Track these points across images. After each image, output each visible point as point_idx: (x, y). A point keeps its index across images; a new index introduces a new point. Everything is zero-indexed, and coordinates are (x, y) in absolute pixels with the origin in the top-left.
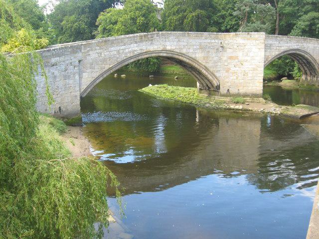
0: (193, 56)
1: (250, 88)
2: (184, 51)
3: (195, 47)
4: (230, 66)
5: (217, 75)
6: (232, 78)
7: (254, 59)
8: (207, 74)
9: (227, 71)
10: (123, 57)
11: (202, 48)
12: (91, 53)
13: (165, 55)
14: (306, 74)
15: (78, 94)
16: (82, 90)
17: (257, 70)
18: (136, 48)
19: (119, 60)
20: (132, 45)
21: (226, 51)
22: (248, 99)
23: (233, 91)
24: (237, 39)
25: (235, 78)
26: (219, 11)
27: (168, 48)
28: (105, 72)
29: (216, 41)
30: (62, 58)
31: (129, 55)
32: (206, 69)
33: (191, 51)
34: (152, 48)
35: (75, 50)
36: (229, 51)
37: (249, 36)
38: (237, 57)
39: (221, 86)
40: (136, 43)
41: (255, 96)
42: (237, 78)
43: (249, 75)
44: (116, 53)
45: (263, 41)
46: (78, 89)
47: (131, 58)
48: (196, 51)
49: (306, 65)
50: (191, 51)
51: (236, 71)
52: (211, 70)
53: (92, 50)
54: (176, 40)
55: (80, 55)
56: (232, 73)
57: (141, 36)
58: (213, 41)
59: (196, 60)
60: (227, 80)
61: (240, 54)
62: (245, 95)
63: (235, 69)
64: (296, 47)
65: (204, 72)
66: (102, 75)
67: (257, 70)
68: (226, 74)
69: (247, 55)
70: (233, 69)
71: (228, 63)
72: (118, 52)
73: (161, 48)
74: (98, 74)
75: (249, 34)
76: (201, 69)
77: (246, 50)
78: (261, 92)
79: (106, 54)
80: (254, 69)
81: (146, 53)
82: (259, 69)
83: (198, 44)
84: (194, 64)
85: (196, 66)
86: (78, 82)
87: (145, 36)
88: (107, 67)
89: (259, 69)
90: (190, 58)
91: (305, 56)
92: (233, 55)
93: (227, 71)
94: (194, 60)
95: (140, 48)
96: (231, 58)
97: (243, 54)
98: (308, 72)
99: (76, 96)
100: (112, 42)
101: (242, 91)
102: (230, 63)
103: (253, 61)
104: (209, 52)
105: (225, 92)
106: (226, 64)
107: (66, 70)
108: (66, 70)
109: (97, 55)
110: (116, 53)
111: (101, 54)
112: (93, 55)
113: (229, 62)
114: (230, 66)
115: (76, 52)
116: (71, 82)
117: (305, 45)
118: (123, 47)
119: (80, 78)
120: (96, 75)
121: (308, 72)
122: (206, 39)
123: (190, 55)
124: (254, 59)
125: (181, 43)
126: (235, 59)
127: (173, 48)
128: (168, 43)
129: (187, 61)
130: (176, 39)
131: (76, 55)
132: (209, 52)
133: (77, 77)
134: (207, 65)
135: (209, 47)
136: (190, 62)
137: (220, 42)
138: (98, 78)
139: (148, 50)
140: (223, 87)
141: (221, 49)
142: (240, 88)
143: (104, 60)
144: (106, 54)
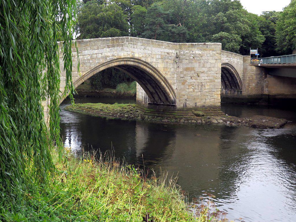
0: (156, 66)
1: (208, 101)
2: (149, 60)
3: (157, 57)
4: (186, 78)
5: (174, 87)
8: (165, 86)
9: (183, 84)
11: (163, 58)
18: (109, 54)
19: (93, 66)
24: (193, 49)
25: (191, 90)
27: (136, 56)
32: (166, 81)
34: (123, 54)
36: (185, 62)
37: (205, 47)
38: (192, 69)
40: (109, 47)
42: (194, 91)
43: (207, 87)
44: (89, 58)
47: (103, 65)
48: (158, 61)
49: (228, 80)
50: (154, 60)
51: (192, 84)
52: (170, 81)
54: (142, 47)
56: (189, 86)
58: (171, 51)
59: (157, 71)
60: (183, 93)
61: (196, 65)
63: (191, 81)
64: (227, 61)
65: (163, 83)
68: (182, 86)
69: (204, 66)
70: (189, 81)
71: (185, 75)
72: (91, 56)
76: (161, 81)
78: (219, 104)
80: (212, 81)
81: (118, 60)
82: (216, 81)
85: (157, 77)
89: (216, 81)
91: (230, 70)
92: (189, 66)
93: (183, 84)
95: (112, 54)
96: (187, 69)
97: (199, 65)
102: (185, 74)
103: (210, 73)
105: (182, 105)
106: (182, 76)
110: (89, 58)
113: (185, 73)
114: (186, 78)
118: (96, 51)
122: (165, 48)
123: (153, 65)
125: (146, 51)
126: (190, 71)
127: (141, 56)
128: (136, 50)
129: (151, 71)
130: (142, 46)
134: (166, 77)
136: (152, 73)
137: (176, 52)
140: (180, 101)
141: (177, 60)
142: (198, 101)
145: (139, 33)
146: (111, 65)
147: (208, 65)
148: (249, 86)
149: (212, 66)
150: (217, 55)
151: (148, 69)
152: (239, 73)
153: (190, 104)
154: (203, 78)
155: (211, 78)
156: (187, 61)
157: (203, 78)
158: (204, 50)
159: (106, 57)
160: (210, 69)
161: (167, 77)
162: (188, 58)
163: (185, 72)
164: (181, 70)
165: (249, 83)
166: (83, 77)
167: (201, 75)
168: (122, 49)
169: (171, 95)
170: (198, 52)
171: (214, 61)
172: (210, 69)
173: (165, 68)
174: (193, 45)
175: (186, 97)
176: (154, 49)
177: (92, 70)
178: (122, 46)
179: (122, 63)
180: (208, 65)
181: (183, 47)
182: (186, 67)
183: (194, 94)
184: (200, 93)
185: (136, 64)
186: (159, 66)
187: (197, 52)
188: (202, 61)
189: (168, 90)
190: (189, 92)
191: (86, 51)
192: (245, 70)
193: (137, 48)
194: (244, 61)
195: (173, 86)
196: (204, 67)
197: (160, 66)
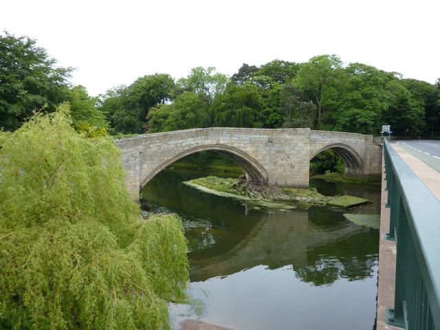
0: (244, 150)
1: (297, 180)
2: (236, 145)
3: (245, 142)
4: (277, 159)
7: (300, 153)
8: (256, 166)
10: (181, 150)
11: (252, 142)
12: (151, 146)
13: (218, 148)
14: (348, 166)
15: (138, 183)
16: (142, 180)
20: (189, 140)
22: (294, 190)
23: (281, 182)
26: (264, 108)
27: (222, 142)
28: (164, 164)
29: (265, 136)
30: (124, 151)
31: (186, 148)
32: (256, 162)
33: (242, 145)
35: (136, 143)
36: (276, 145)
38: (284, 151)
39: (269, 179)
43: (296, 168)
46: (138, 178)
47: (188, 151)
49: (349, 159)
50: (242, 145)
53: (152, 143)
55: (141, 148)
56: (280, 166)
57: (197, 131)
58: (262, 136)
60: (275, 172)
61: (287, 148)
62: (294, 187)
64: (338, 142)
65: (254, 164)
66: (160, 166)
70: (280, 162)
72: (176, 145)
73: (215, 142)
74: (157, 165)
76: (251, 162)
77: (292, 145)
79: (164, 146)
80: (301, 162)
82: (305, 162)
83: (248, 139)
84: (245, 158)
85: (247, 159)
86: (138, 172)
87: (200, 131)
88: (166, 159)
89: (305, 162)
90: (241, 152)
92: (281, 149)
94: (245, 154)
96: (278, 152)
98: (350, 164)
99: (136, 186)
100: (172, 137)
101: (289, 182)
104: (258, 146)
106: (274, 157)
107: (128, 161)
108: (128, 161)
109: (157, 148)
111: (160, 146)
112: (154, 148)
114: (277, 159)
115: (138, 145)
116: (132, 172)
117: (347, 140)
118: (181, 141)
119: (141, 169)
120: (155, 166)
121: (350, 164)
122: (255, 134)
123: (241, 149)
128: (221, 138)
129: (239, 154)
131: (137, 148)
132: (258, 146)
133: (138, 168)
134: (256, 159)
135: (258, 142)
136: (241, 156)
138: (157, 169)
139: (203, 144)
141: (269, 143)
143: (163, 153)
144: (164, 146)
145: (226, 124)
146: (196, 151)
147: (298, 149)
148: (370, 165)
149: (302, 148)
151: (236, 153)
152: (359, 153)
155: (300, 160)
156: (278, 145)
158: (294, 135)
159: (190, 145)
160: (299, 152)
161: (258, 158)
163: (277, 155)
164: (273, 152)
165: (370, 162)
166: (170, 160)
167: (291, 157)
168: (207, 138)
169: (263, 174)
170: (288, 137)
171: (303, 145)
172: (299, 152)
173: (256, 152)
175: (277, 176)
176: (242, 136)
177: (177, 156)
178: (207, 135)
179: (208, 149)
180: (298, 149)
185: (224, 149)
186: (248, 150)
189: (260, 170)
191: (171, 142)
192: (367, 148)
193: (222, 136)
194: (366, 139)
195: (264, 167)
196: (293, 149)
197: (249, 150)
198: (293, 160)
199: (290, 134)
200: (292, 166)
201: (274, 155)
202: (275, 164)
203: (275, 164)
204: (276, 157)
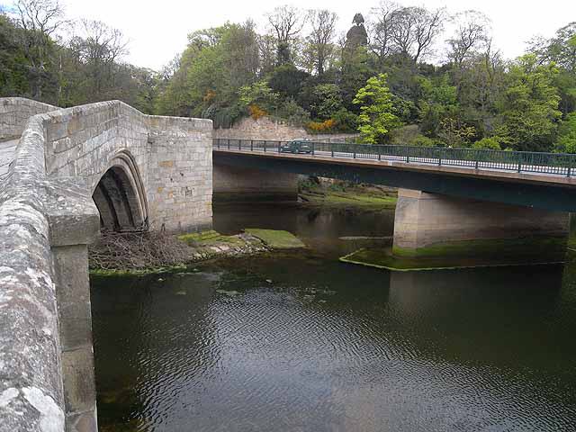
1: (196, 216)
6: (167, 202)
17: (204, 184)
21: (155, 151)
36: (160, 150)
39: (150, 221)
41: (201, 228)
43: (194, 194)
45: (209, 134)
60: (160, 207)
61: (179, 157)
67: (204, 184)
68: (158, 195)
75: (190, 120)
80: (200, 183)
89: (206, 182)
96: (164, 164)
103: (197, 169)
124: (200, 166)
150: (207, 139)
153: (171, 225)
154: (190, 179)
155: (199, 178)
157: (188, 179)
158: (190, 129)
162: (165, 144)
163: (162, 170)
164: (155, 166)
170: (181, 134)
171: (203, 150)
174: (174, 119)
181: (157, 122)
182: (162, 160)
183: (175, 208)
184: (184, 205)
187: (181, 134)
188: (187, 150)
190: (168, 204)
196: (189, 159)
198: (190, 179)
199: (183, 128)
200: (188, 192)
201: (156, 170)
202: (160, 189)
203: (160, 189)
204: (162, 175)
